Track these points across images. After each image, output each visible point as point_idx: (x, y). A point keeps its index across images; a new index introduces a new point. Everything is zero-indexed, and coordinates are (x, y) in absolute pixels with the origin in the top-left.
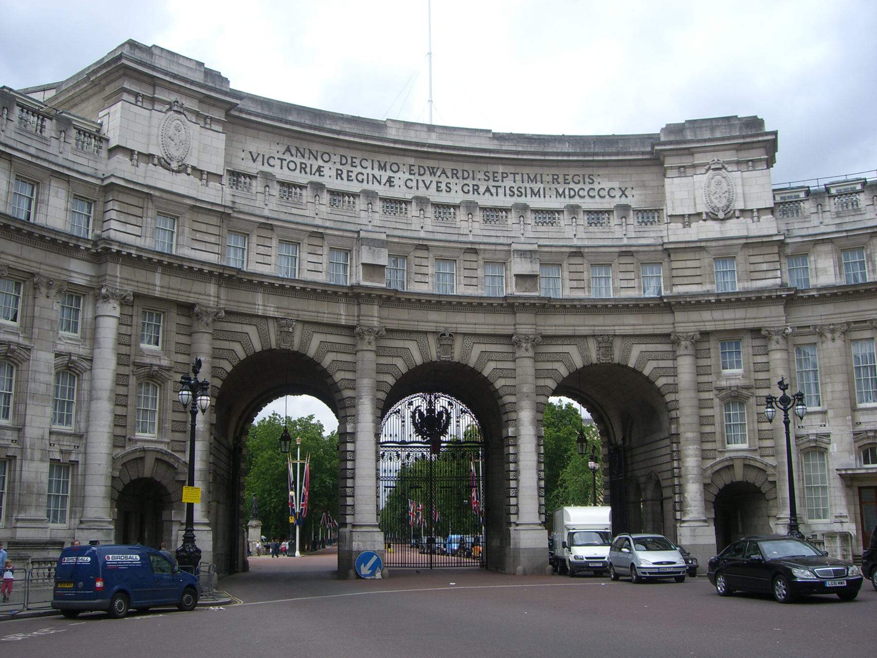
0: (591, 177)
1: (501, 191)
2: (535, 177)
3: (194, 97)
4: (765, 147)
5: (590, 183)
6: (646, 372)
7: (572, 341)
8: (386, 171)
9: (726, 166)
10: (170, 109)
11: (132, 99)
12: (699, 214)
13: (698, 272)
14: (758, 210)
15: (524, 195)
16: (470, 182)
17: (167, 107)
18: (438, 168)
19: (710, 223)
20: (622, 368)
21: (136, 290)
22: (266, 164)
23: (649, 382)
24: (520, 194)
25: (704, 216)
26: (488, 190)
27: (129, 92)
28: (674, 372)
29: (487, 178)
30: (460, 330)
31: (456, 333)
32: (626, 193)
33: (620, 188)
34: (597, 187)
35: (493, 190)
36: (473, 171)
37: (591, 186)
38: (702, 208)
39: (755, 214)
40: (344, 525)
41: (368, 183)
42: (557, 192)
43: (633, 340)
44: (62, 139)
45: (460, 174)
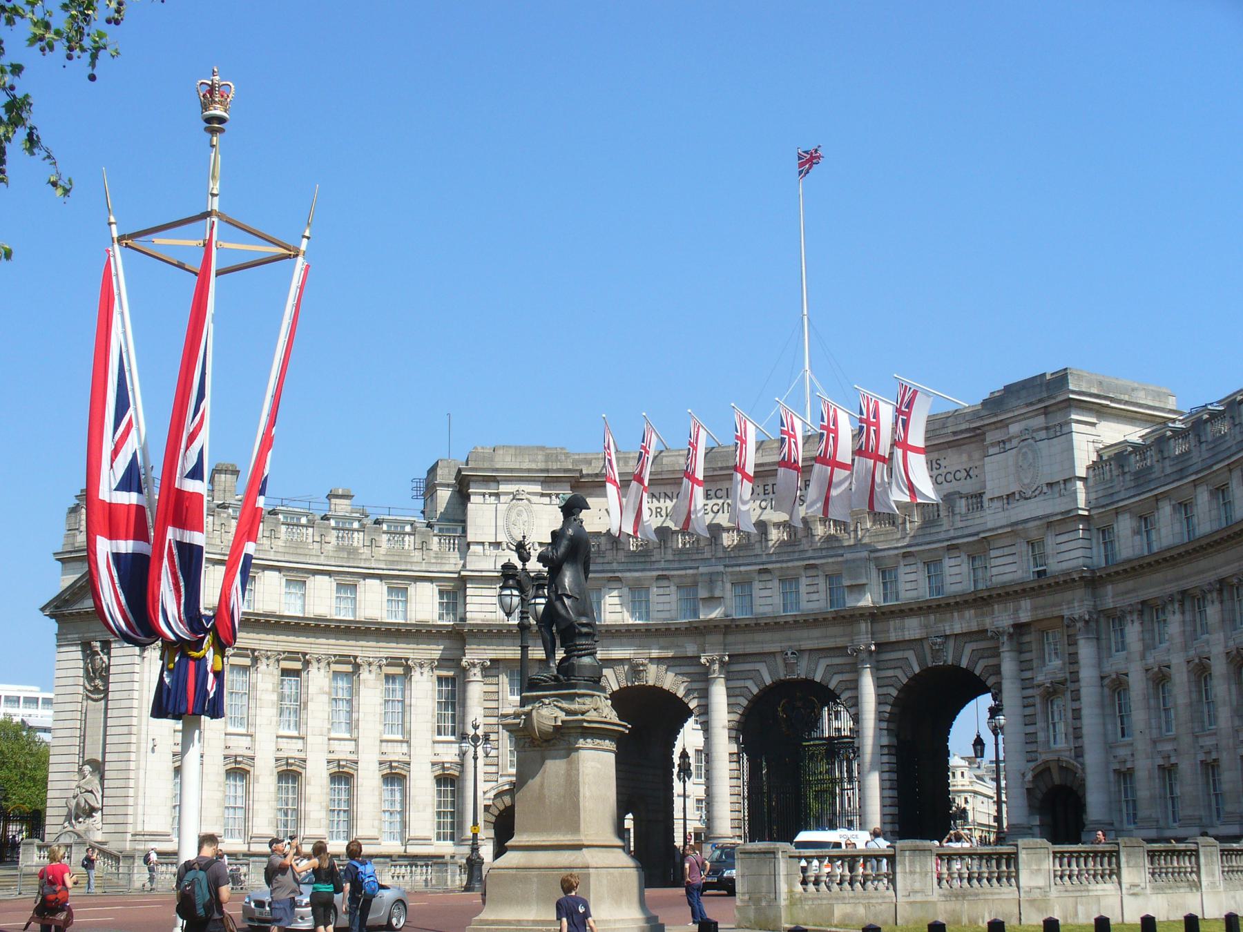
3: (539, 481)
4: (1070, 406)
6: (977, 672)
9: (1034, 435)
10: (513, 499)
11: (479, 499)
12: (1014, 493)
14: (1065, 481)
17: (511, 496)
19: (1022, 502)
20: (956, 669)
21: (493, 657)
25: (1017, 497)
27: (475, 494)
30: (803, 647)
31: (801, 651)
32: (971, 473)
33: (965, 470)
34: (943, 471)
38: (1014, 488)
39: (1062, 486)
44: (424, 548)
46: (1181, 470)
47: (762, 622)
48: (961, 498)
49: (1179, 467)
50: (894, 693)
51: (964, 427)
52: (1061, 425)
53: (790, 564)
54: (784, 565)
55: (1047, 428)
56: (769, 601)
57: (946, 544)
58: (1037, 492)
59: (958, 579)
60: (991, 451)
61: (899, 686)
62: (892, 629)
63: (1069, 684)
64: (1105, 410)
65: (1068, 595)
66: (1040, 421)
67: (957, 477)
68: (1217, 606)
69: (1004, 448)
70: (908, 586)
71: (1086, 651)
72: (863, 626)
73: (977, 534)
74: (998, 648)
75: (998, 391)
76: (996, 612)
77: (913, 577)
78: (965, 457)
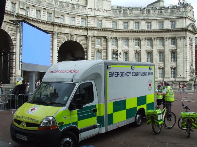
6: (81, 43)
7: (65, 34)
12: (95, 9)
13: (94, 22)
20: (75, 42)
23: (81, 46)
25: (96, 10)
28: (87, 44)
40: (12, 76)
43: (79, 36)
46: (137, 17)
47: (34, 19)
49: (137, 16)
50: (61, 45)
53: (40, 7)
54: (39, 6)
56: (33, 14)
57: (78, 14)
59: (79, 23)
61: (62, 43)
62: (62, 30)
63: (103, 50)
65: (107, 33)
68: (144, 42)
70: (67, 21)
71: (110, 44)
72: (56, 28)
73: (87, 15)
74: (87, 39)
76: (88, 32)
77: (68, 19)
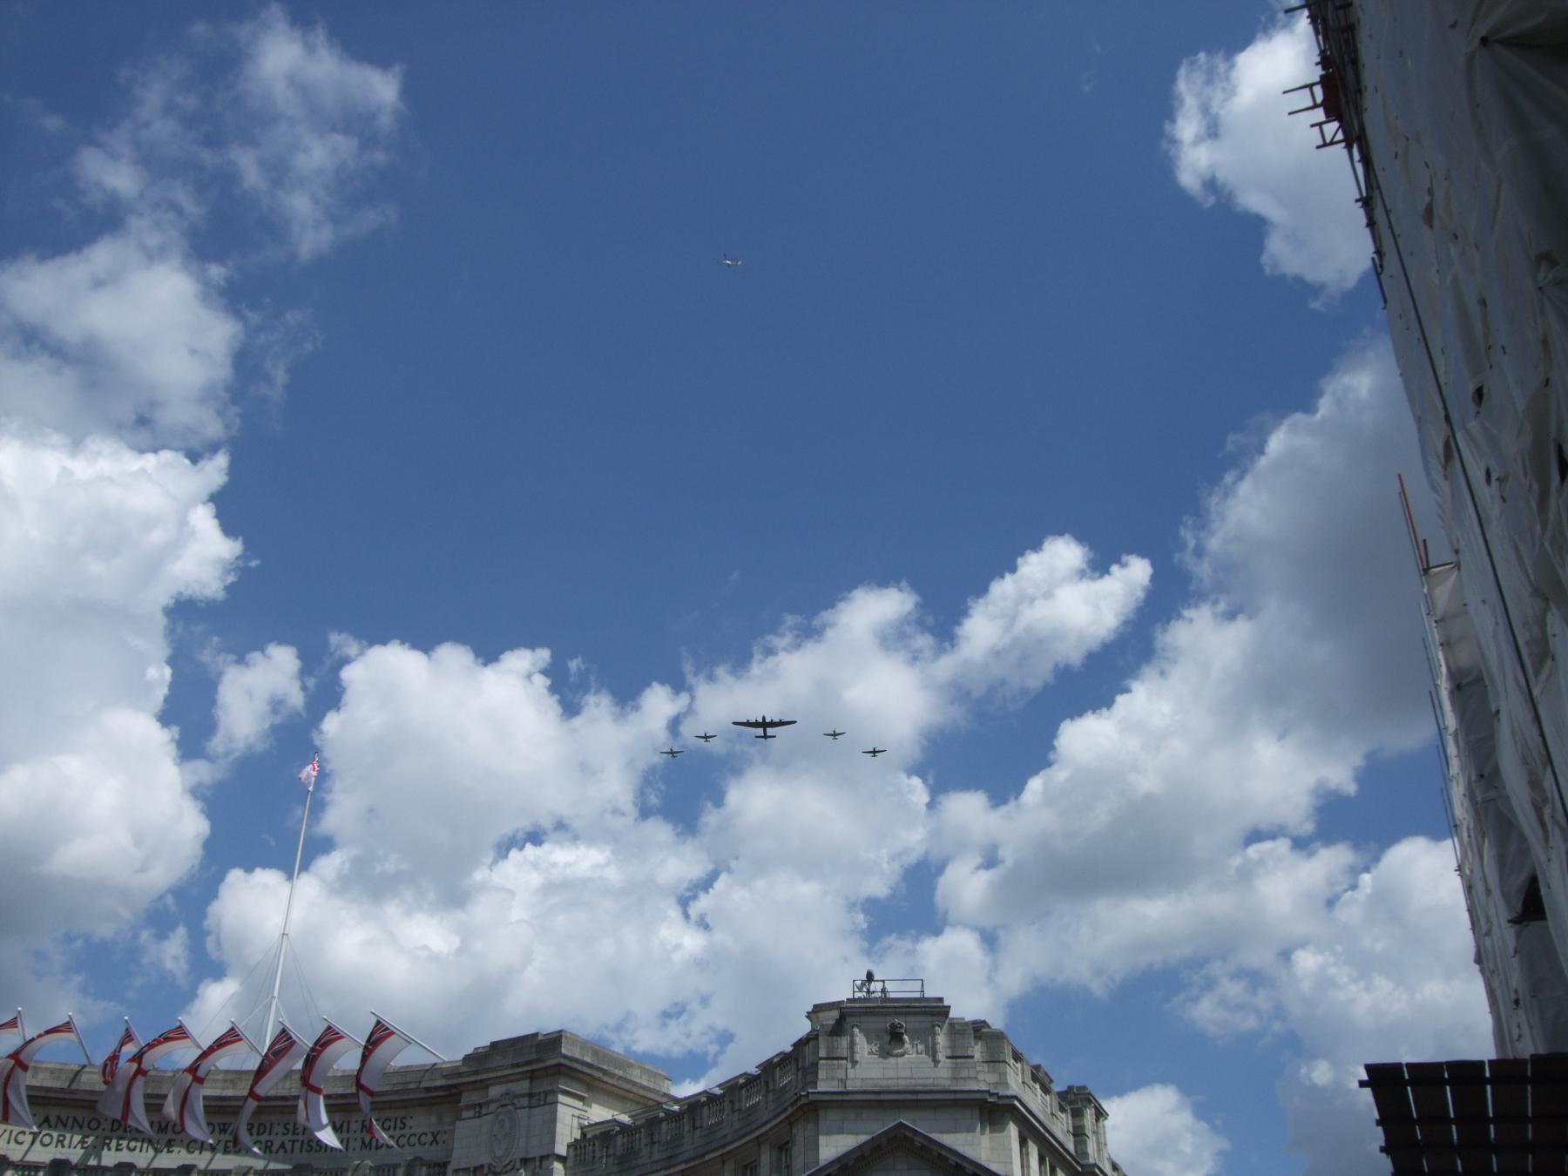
0: (404, 1121)
1: (298, 1145)
2: (342, 1126)
5: (401, 1129)
8: (166, 1133)
9: (516, 1101)
12: (482, 1166)
15: (323, 1150)
16: (264, 1138)
18: (231, 1124)
22: (12, 1143)
24: (318, 1149)
25: (486, 1170)
26: (282, 1146)
29: (286, 1132)
32: (438, 1138)
33: (433, 1133)
34: (407, 1131)
35: (288, 1146)
36: (271, 1125)
37: (402, 1132)
39: (538, 1163)
41: (141, 1151)
42: (363, 1142)
45: (254, 1131)
48: (422, 1165)
51: (439, 1083)
52: (546, 1094)
55: (531, 1095)
58: (509, 1167)
60: (465, 1114)
64: (597, 1083)
66: (524, 1086)
67: (423, 1139)
69: (480, 1113)
75: (484, 1047)
78: (434, 1119)
